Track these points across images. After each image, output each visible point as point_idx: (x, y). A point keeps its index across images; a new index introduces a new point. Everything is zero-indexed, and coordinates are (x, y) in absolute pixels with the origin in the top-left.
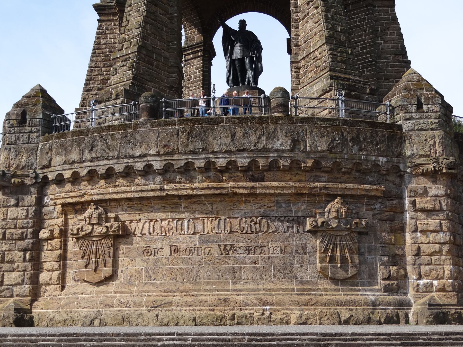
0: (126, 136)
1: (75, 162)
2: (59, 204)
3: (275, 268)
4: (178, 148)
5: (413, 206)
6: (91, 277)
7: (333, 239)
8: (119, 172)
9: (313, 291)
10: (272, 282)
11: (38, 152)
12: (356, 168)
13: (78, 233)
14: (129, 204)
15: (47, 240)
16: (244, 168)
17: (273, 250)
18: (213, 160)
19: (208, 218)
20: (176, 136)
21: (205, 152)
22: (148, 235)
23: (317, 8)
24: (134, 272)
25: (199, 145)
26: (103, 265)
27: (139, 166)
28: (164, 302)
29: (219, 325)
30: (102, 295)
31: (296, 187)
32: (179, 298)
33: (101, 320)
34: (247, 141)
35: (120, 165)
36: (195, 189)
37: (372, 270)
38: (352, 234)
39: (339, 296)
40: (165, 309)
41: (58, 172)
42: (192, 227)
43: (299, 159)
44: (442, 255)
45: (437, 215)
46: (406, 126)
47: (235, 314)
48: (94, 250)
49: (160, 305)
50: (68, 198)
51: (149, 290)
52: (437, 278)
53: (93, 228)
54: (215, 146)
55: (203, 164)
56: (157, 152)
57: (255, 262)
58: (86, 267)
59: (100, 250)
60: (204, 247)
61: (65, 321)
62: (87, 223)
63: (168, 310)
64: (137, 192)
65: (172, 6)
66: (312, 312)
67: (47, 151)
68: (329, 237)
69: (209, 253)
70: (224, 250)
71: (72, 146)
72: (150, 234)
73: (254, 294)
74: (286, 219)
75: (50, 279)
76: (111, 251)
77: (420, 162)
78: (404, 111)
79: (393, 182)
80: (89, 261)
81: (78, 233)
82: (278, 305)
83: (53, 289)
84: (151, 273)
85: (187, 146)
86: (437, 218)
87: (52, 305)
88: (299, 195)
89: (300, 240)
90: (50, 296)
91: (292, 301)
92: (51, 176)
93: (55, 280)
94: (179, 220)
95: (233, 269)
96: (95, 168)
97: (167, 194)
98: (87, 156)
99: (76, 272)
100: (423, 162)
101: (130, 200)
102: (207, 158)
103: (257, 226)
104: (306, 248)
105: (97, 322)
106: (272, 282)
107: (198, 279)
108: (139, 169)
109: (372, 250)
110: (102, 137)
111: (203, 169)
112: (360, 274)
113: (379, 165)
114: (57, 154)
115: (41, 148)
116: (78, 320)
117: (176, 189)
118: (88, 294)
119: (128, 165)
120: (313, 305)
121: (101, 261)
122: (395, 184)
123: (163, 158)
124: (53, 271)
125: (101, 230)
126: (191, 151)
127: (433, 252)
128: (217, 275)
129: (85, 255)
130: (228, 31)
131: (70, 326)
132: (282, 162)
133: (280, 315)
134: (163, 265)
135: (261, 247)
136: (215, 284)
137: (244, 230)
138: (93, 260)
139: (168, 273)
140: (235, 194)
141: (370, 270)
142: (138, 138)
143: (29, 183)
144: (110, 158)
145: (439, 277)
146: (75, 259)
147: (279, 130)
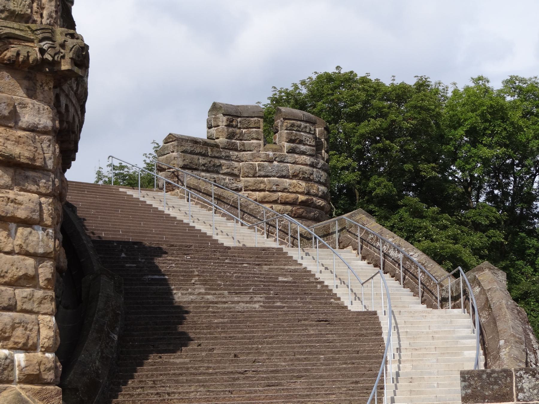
44: (36, 286)
45: (36, 183)
52: (26, 348)
77: (13, 31)
86: (34, 188)
100: (18, 32)
127: (20, 278)
145: (30, 343)
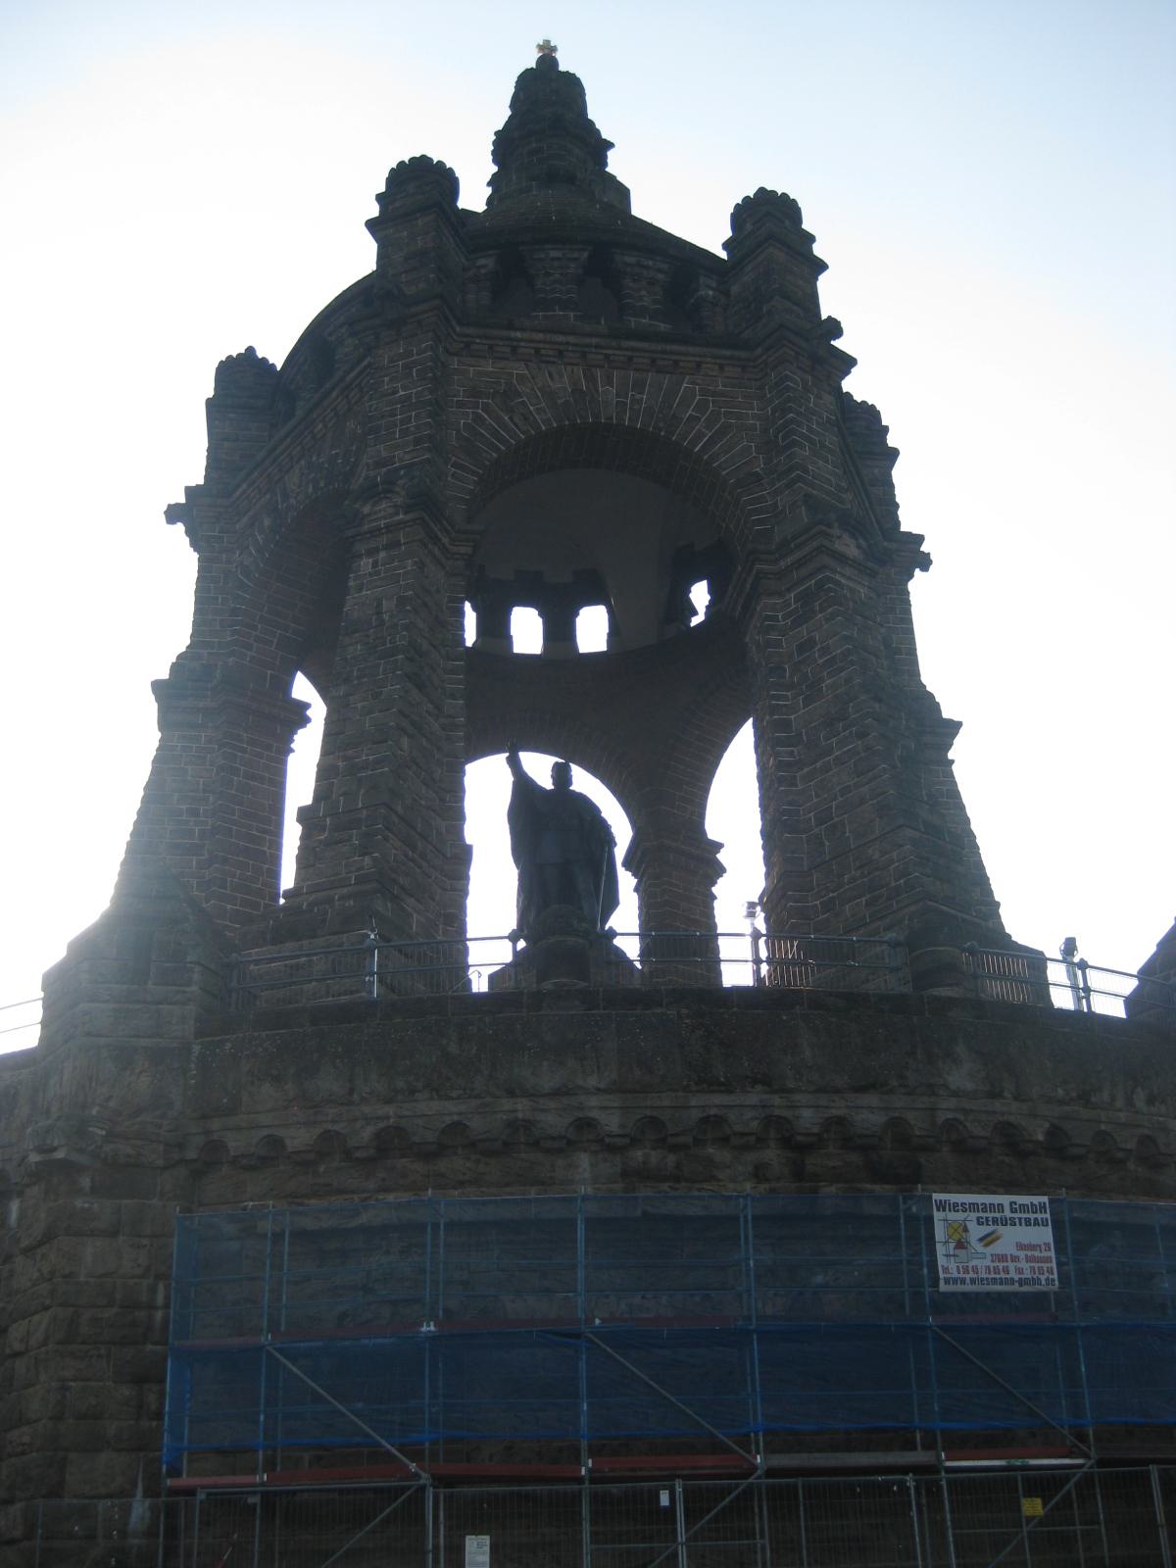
23: (862, 735)
41: (265, 1132)
43: (1012, 1119)
55: (755, 1124)
65: (453, 696)
92: (235, 1143)
111: (752, 1139)
130: (523, 785)
143: (160, 1162)
144: (454, 1094)
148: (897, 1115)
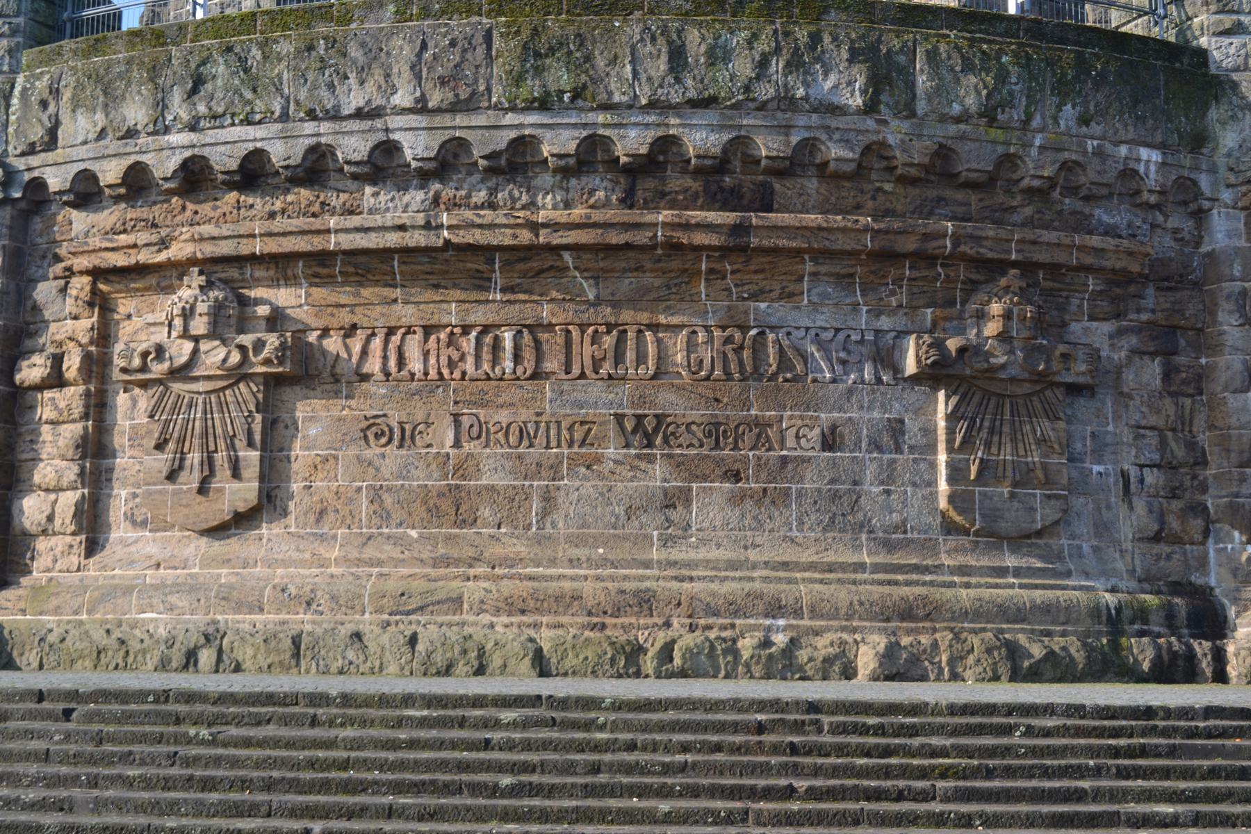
0: (311, 48)
1: (137, 132)
2: (81, 273)
3: (800, 494)
4: (489, 89)
5: (1238, 311)
6: (186, 511)
7: (991, 406)
8: (286, 167)
9: (922, 573)
10: (793, 541)
11: (15, 101)
12: (1065, 179)
13: (144, 368)
14: (316, 275)
15: (41, 387)
16: (708, 162)
17: (797, 437)
18: (607, 132)
19: (583, 327)
20: (481, 51)
21: (580, 103)
22: (381, 377)
24: (330, 496)
25: (560, 77)
26: (228, 473)
27: (354, 145)
28: (436, 598)
29: (620, 676)
30: (225, 571)
31: (879, 231)
32: (486, 585)
33: (220, 651)
34: (722, 75)
35: (291, 142)
36: (544, 225)
37: (1104, 511)
38: (1048, 393)
39: (1010, 592)
40: (440, 619)
41: (82, 166)
42: (528, 355)
46: (1223, 53)
47: (674, 642)
48: (197, 423)
49: (421, 609)
50: (113, 249)
51: (383, 557)
53: (195, 352)
54: (613, 86)
55: (571, 147)
56: (417, 101)
57: (737, 477)
58: (172, 476)
59: (217, 423)
60: (569, 420)
61: (99, 653)
62: (174, 334)
63: (450, 625)
64: (347, 231)
66: (925, 640)
67: (46, 94)
68: (976, 400)
69: (584, 440)
70: (634, 431)
71: (125, 76)
72: (387, 374)
73: (734, 579)
74: (841, 336)
75: (50, 518)
76: (257, 428)
78: (1213, 8)
79: (1176, 231)
80: (182, 460)
81: (144, 368)
82: (815, 613)
83: (60, 548)
84: (388, 500)
85: (519, 80)
87: (54, 602)
88: (886, 257)
89: (884, 408)
90: (48, 570)
91: (861, 604)
93: (68, 521)
94: (486, 329)
95: (666, 495)
96: (206, 152)
97: (447, 242)
98: (178, 108)
99: (135, 496)
101: (322, 258)
102: (585, 126)
103: (746, 354)
104: (903, 434)
105: (206, 657)
106: (793, 541)
107: (548, 525)
108: (357, 157)
109: (1107, 445)
110: (229, 49)
111: (572, 161)
112: (1068, 523)
113: (1136, 172)
114: (76, 105)
115: (24, 90)
116: (144, 652)
117: (480, 226)
118: (176, 568)
119: (319, 145)
120: (927, 617)
121: (221, 458)
122: (1182, 239)
123: (438, 121)
124: (58, 489)
125: (222, 356)
126: (535, 100)
128: (613, 514)
129: (166, 441)
131: (116, 667)
132: (835, 151)
133: (823, 645)
134: (429, 477)
135: (756, 425)
136: (605, 544)
137: (701, 369)
138: (194, 457)
139: (446, 505)
140: (674, 247)
141: (1099, 509)
142: (355, 52)
144: (258, 117)
146: (135, 452)
147: (827, 39)
148: (743, 133)
